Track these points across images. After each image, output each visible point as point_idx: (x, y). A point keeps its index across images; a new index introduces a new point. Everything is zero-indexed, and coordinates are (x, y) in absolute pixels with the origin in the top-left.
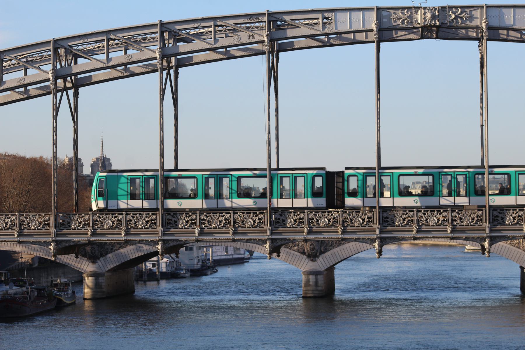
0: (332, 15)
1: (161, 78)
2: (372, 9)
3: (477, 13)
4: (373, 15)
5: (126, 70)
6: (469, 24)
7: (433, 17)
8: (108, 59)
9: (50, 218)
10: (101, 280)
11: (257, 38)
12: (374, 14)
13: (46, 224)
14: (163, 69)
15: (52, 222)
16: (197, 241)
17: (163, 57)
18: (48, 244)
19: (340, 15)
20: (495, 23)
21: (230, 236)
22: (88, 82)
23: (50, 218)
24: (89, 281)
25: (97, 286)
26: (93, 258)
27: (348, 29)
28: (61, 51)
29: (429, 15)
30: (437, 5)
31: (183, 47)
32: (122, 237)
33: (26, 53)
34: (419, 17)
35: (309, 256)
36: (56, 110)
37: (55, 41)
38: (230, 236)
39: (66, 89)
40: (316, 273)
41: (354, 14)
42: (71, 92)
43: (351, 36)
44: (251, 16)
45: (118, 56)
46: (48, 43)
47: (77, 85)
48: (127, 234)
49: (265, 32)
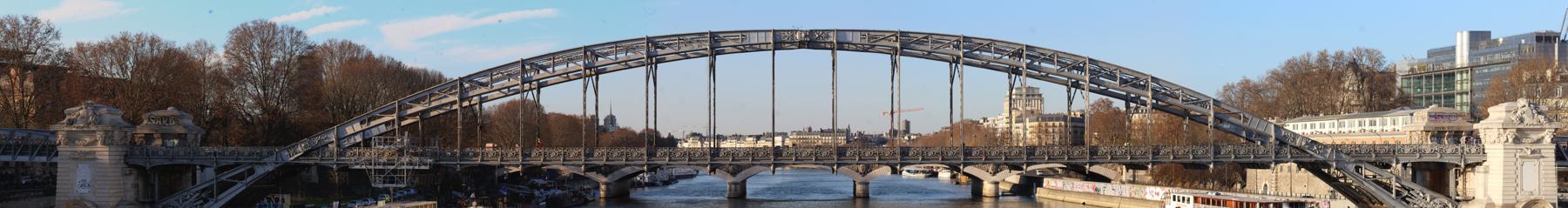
0: (747, 34)
2: (770, 31)
3: (831, 34)
7: (806, 36)
8: (616, 58)
9: (582, 150)
10: (610, 187)
11: (703, 47)
12: (771, 34)
13: (580, 154)
15: (583, 153)
16: (668, 165)
17: (648, 58)
19: (752, 34)
20: (841, 40)
21: (686, 162)
23: (582, 150)
25: (608, 190)
26: (606, 174)
27: (756, 42)
28: (589, 53)
29: (803, 35)
31: (660, 51)
32: (624, 162)
33: (568, 54)
34: (797, 36)
35: (731, 174)
36: (962, 115)
37: (585, 47)
38: (686, 162)
39: (591, 75)
40: (735, 184)
41: (760, 34)
42: (594, 77)
43: (758, 46)
45: (621, 56)
46: (581, 48)
47: (597, 74)
48: (627, 160)
49: (708, 44)
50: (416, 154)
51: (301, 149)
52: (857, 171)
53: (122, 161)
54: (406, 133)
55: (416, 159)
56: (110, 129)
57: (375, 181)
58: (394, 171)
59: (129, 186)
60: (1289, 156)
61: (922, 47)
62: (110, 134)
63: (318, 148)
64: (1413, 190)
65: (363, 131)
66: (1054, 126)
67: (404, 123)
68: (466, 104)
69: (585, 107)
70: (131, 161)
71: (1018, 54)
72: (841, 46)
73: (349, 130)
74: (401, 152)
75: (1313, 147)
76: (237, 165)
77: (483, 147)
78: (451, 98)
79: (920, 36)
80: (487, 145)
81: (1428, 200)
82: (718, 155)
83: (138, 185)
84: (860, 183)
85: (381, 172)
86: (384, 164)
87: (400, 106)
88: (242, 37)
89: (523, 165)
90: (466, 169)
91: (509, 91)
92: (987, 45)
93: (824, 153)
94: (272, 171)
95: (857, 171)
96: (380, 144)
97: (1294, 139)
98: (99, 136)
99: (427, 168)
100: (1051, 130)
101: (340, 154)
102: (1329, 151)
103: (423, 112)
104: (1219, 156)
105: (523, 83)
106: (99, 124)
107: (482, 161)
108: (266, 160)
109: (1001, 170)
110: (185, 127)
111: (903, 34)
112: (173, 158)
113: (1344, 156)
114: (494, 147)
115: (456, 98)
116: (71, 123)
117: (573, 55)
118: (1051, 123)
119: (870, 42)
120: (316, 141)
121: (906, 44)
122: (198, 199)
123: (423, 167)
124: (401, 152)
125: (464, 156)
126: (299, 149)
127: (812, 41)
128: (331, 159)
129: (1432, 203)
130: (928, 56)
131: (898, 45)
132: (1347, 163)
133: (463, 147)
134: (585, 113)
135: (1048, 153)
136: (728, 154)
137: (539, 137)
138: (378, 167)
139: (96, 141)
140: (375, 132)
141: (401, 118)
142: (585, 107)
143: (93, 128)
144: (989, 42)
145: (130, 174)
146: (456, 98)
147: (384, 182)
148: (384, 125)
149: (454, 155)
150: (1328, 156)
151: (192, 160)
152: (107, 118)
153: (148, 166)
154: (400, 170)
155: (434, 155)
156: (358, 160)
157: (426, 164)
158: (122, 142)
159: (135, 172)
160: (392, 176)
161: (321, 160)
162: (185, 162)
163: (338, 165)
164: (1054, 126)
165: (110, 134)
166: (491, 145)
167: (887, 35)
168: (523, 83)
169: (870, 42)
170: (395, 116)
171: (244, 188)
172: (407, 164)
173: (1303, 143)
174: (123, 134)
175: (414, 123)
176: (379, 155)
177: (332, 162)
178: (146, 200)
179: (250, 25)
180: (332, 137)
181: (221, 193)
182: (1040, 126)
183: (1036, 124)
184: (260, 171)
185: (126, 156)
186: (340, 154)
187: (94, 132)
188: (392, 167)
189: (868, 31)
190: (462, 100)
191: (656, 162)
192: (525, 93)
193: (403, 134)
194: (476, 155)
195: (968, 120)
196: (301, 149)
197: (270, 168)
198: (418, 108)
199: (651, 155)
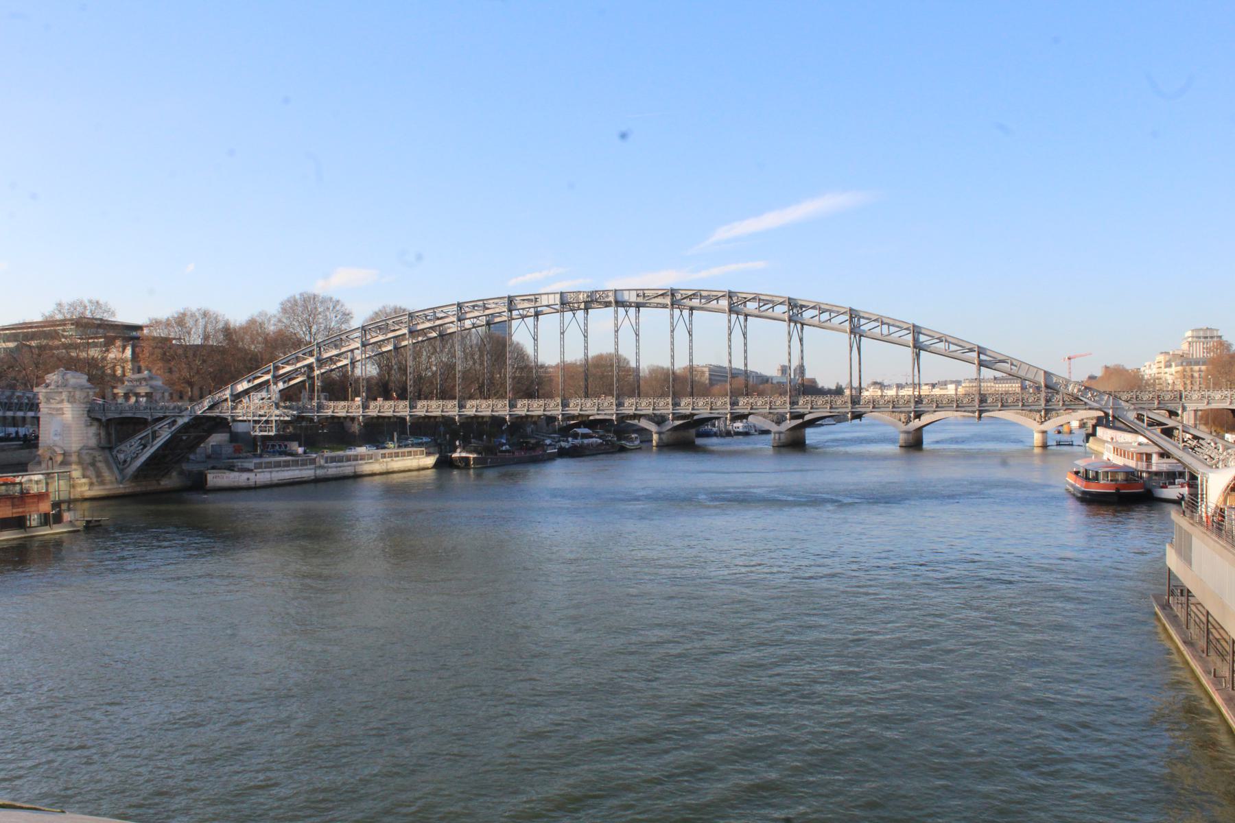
4: (558, 296)
7: (588, 296)
9: (407, 403)
10: (662, 436)
18: (613, 414)
21: (768, 411)
24: (655, 437)
25: (660, 439)
32: (595, 412)
34: (581, 296)
35: (776, 423)
38: (768, 411)
40: (780, 433)
48: (598, 410)
51: (206, 403)
52: (900, 420)
53: (86, 415)
56: (70, 390)
58: (267, 422)
59: (90, 435)
60: (1061, 403)
62: (72, 394)
64: (1203, 439)
69: (673, 357)
70: (93, 415)
75: (1086, 394)
77: (353, 400)
81: (1221, 450)
82: (858, 403)
83: (99, 434)
84: (656, 433)
88: (290, 308)
89: (617, 414)
94: (188, 423)
95: (900, 420)
97: (1066, 386)
98: (64, 396)
99: (289, 419)
100: (1196, 375)
104: (984, 404)
106: (65, 386)
108: (184, 413)
109: (1049, 419)
110: (151, 387)
112: (121, 413)
113: (1123, 404)
116: (47, 386)
118: (1196, 368)
122: (141, 444)
123: (286, 418)
129: (1225, 453)
132: (1129, 410)
134: (673, 364)
135: (1023, 399)
139: (63, 400)
142: (673, 357)
143: (60, 390)
145: (91, 425)
147: (261, 431)
150: (1104, 403)
151: (135, 413)
152: (72, 381)
153: (104, 419)
155: (298, 409)
158: (86, 400)
159: (96, 423)
161: (221, 412)
162: (129, 415)
165: (72, 394)
173: (1075, 391)
174: (85, 394)
179: (298, 297)
180: (227, 394)
182: (1184, 371)
183: (1180, 368)
185: (89, 411)
187: (61, 392)
188: (264, 419)
189: (643, 290)
195: (735, 369)
196: (206, 403)
197: (186, 420)
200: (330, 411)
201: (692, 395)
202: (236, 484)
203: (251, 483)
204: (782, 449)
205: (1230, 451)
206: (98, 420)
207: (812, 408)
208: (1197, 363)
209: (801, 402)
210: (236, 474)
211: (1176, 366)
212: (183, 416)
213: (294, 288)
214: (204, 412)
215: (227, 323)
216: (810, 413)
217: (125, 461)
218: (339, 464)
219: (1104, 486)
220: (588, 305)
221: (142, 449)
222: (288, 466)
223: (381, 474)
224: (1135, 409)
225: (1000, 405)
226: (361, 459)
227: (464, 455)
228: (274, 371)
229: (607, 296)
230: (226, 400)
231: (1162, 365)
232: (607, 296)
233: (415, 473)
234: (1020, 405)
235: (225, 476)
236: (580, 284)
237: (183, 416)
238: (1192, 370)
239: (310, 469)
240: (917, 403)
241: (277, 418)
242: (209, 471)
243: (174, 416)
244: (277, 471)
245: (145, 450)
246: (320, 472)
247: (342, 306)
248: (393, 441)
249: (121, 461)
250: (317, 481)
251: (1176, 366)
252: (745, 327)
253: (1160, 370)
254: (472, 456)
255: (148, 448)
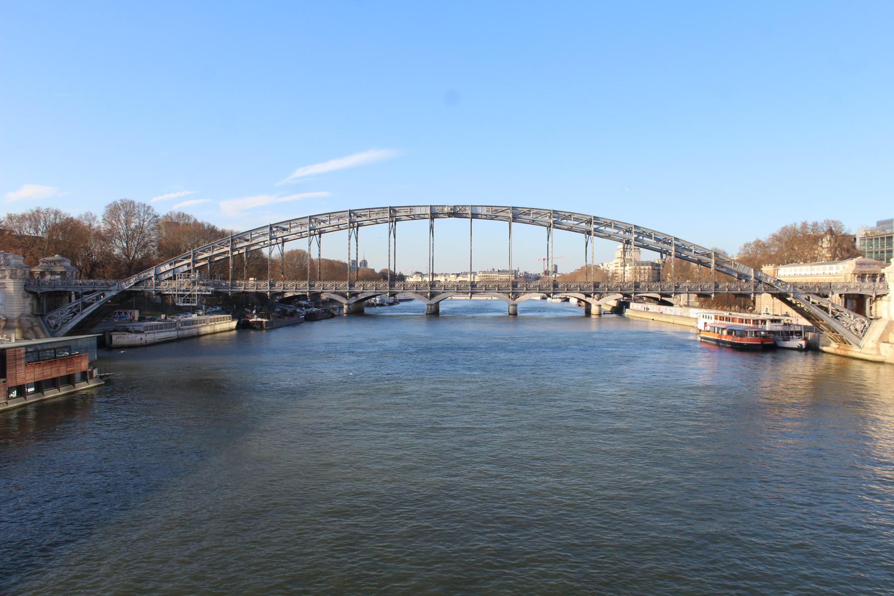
0: (414, 208)
1: (349, 232)
3: (467, 208)
5: (339, 227)
6: (464, 212)
7: (451, 209)
8: (330, 223)
9: (307, 282)
11: (385, 216)
12: (429, 207)
13: (306, 285)
14: (350, 228)
15: (308, 284)
16: (362, 292)
17: (350, 223)
19: (416, 208)
20: (474, 212)
22: (324, 232)
23: (307, 282)
24: (345, 307)
25: (349, 308)
28: (313, 220)
29: (449, 209)
30: (453, 205)
31: (359, 219)
33: (301, 221)
37: (310, 216)
39: (315, 235)
40: (431, 305)
42: (318, 236)
44: (383, 208)
45: (333, 222)
47: (320, 233)
50: (203, 285)
51: (133, 281)
54: (198, 271)
55: (203, 288)
56: (14, 268)
57: (178, 302)
58: (190, 295)
59: (27, 305)
60: (763, 290)
61: (527, 217)
63: (144, 281)
65: (174, 269)
66: (644, 269)
67: (197, 265)
68: (236, 253)
70: (29, 289)
71: (589, 222)
72: (475, 216)
73: (163, 269)
74: (194, 283)
76: (94, 291)
77: (248, 279)
78: (226, 249)
79: (525, 210)
80: (251, 279)
85: (182, 296)
86: (184, 291)
87: (194, 254)
88: (114, 211)
90: (235, 294)
91: (264, 244)
92: (569, 216)
93: (463, 286)
94: (116, 295)
96: (181, 278)
97: (766, 278)
98: (7, 273)
99: (210, 293)
100: (642, 271)
101: (157, 284)
102: (789, 286)
103: (211, 257)
105: (271, 239)
106: (8, 265)
107: (244, 289)
108: (111, 288)
110: (65, 267)
111: (513, 208)
113: (798, 289)
114: (254, 280)
115: (229, 249)
117: (303, 221)
118: (642, 267)
119: (494, 214)
120: (142, 276)
121: (516, 215)
123: (207, 293)
124: (194, 283)
125: (233, 286)
126: (132, 281)
127: (455, 213)
128: (150, 288)
130: (533, 222)
131: (511, 215)
132: (801, 294)
133: (234, 279)
136: (414, 285)
137: (283, 273)
138: (180, 293)
139: (6, 276)
140: (181, 270)
141: (195, 262)
144: (569, 214)
145: (28, 297)
146: (229, 249)
147: (184, 302)
148: (186, 266)
149: (227, 286)
150: (788, 289)
152: (13, 261)
153: (39, 292)
154: (194, 295)
156: (167, 287)
157: (209, 291)
158: (23, 276)
159: (31, 296)
160: (188, 298)
162: (62, 289)
163: (156, 291)
164: (644, 269)
165: (14, 271)
166: (253, 279)
167: (504, 209)
168: (271, 239)
169: (494, 214)
170: (190, 261)
171: (98, 306)
172: (198, 291)
173: (772, 281)
174: (23, 272)
175: (205, 265)
176: (181, 285)
177: (152, 289)
178: (38, 313)
179: (119, 202)
180: (152, 273)
181: (84, 309)
182: (636, 269)
184: (108, 295)
185: (25, 285)
186: (157, 284)
187: (4, 270)
188: (188, 293)
190: (233, 250)
191: (354, 290)
192: (273, 246)
193: (196, 272)
194: (240, 285)
196: (133, 281)
197: (114, 293)
198: (205, 255)
199: (351, 285)
200: (243, 287)
201: (320, 280)
202: (133, 343)
203: (143, 342)
204: (433, 316)
205: (857, 319)
206: (34, 294)
207: (404, 289)
208: (643, 264)
209: (397, 285)
210: (134, 335)
211: (630, 266)
212: (111, 290)
213: (117, 197)
214: (130, 287)
215: (196, 221)
216: (443, 292)
217: (56, 326)
218: (189, 327)
219: (751, 340)
220: (434, 216)
221: (73, 316)
222: (161, 328)
223: (211, 334)
224: (805, 293)
225: (647, 289)
226: (200, 323)
227: (259, 320)
228: (194, 257)
229: (465, 210)
230: (150, 278)
231: (619, 265)
232: (465, 210)
233: (228, 334)
234: (579, 289)
235: (125, 336)
236: (449, 201)
237: (111, 290)
238: (640, 269)
239: (174, 331)
240: (636, 287)
241: (200, 293)
242: (114, 333)
243: (102, 290)
244: (158, 332)
245: (75, 317)
246: (180, 333)
247: (153, 210)
248: (202, 310)
249: (52, 326)
250: (179, 339)
251: (630, 266)
252: (357, 233)
253: (617, 268)
254: (264, 320)
255: (78, 315)
